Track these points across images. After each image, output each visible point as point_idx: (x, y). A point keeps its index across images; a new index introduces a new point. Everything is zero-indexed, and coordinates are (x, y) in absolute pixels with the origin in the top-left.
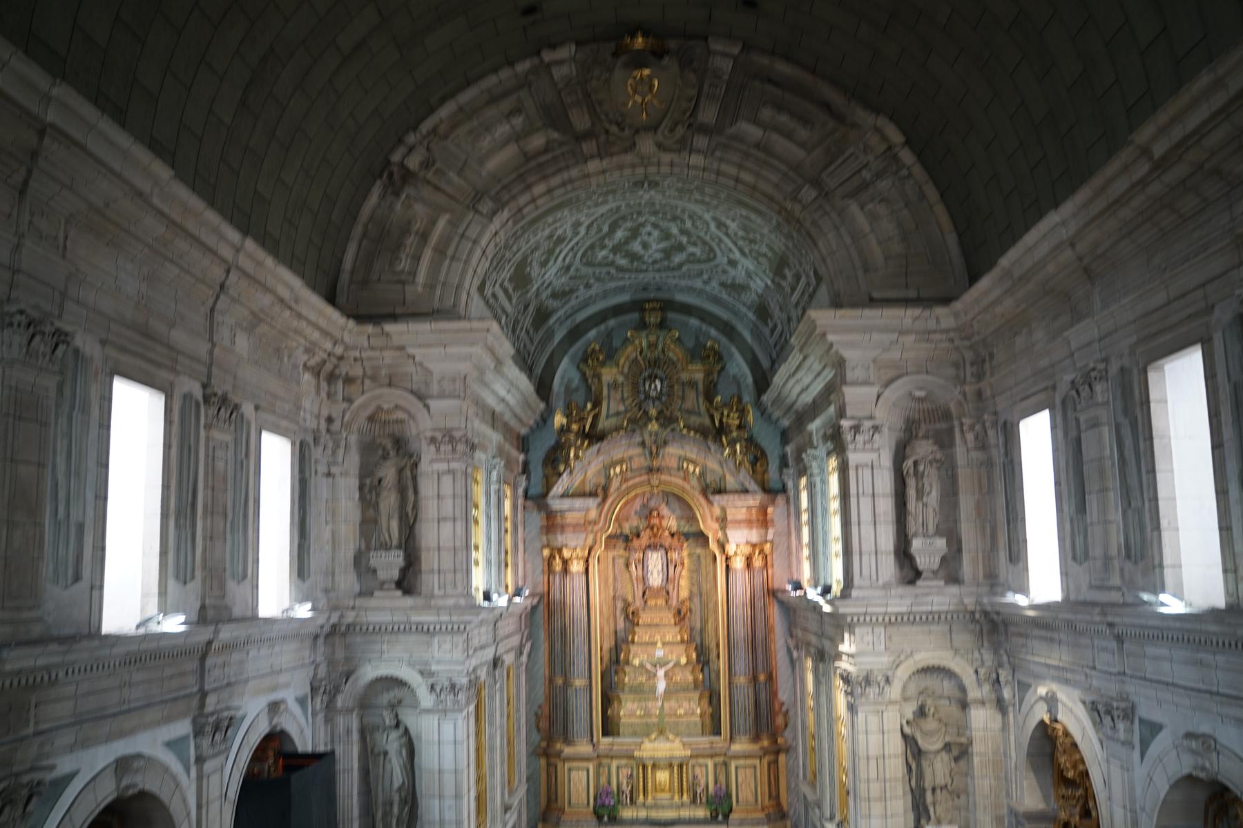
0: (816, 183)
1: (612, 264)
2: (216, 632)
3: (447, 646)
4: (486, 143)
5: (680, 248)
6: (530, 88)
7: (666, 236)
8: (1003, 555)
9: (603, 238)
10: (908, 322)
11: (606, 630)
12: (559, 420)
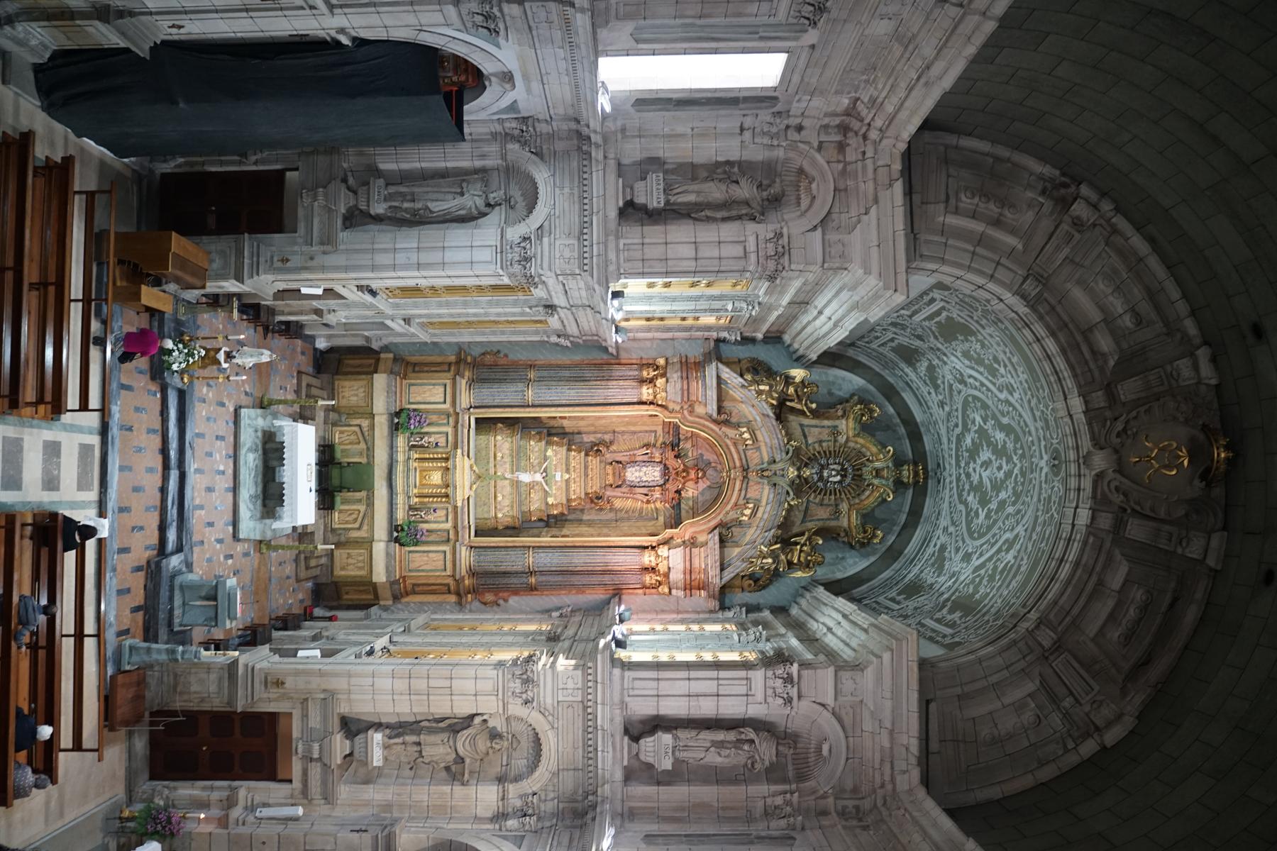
0: (1058, 647)
2: (582, 10)
3: (567, 254)
4: (1102, 286)
5: (984, 502)
6: (1167, 334)
7: (997, 487)
8: (653, 828)
9: (994, 417)
10: (904, 739)
11: (582, 423)
12: (798, 374)
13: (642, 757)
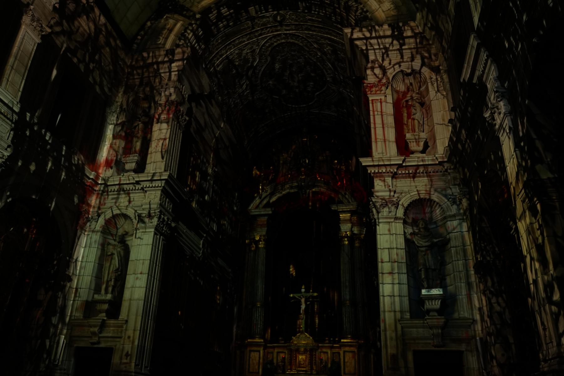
13: (421, 148)
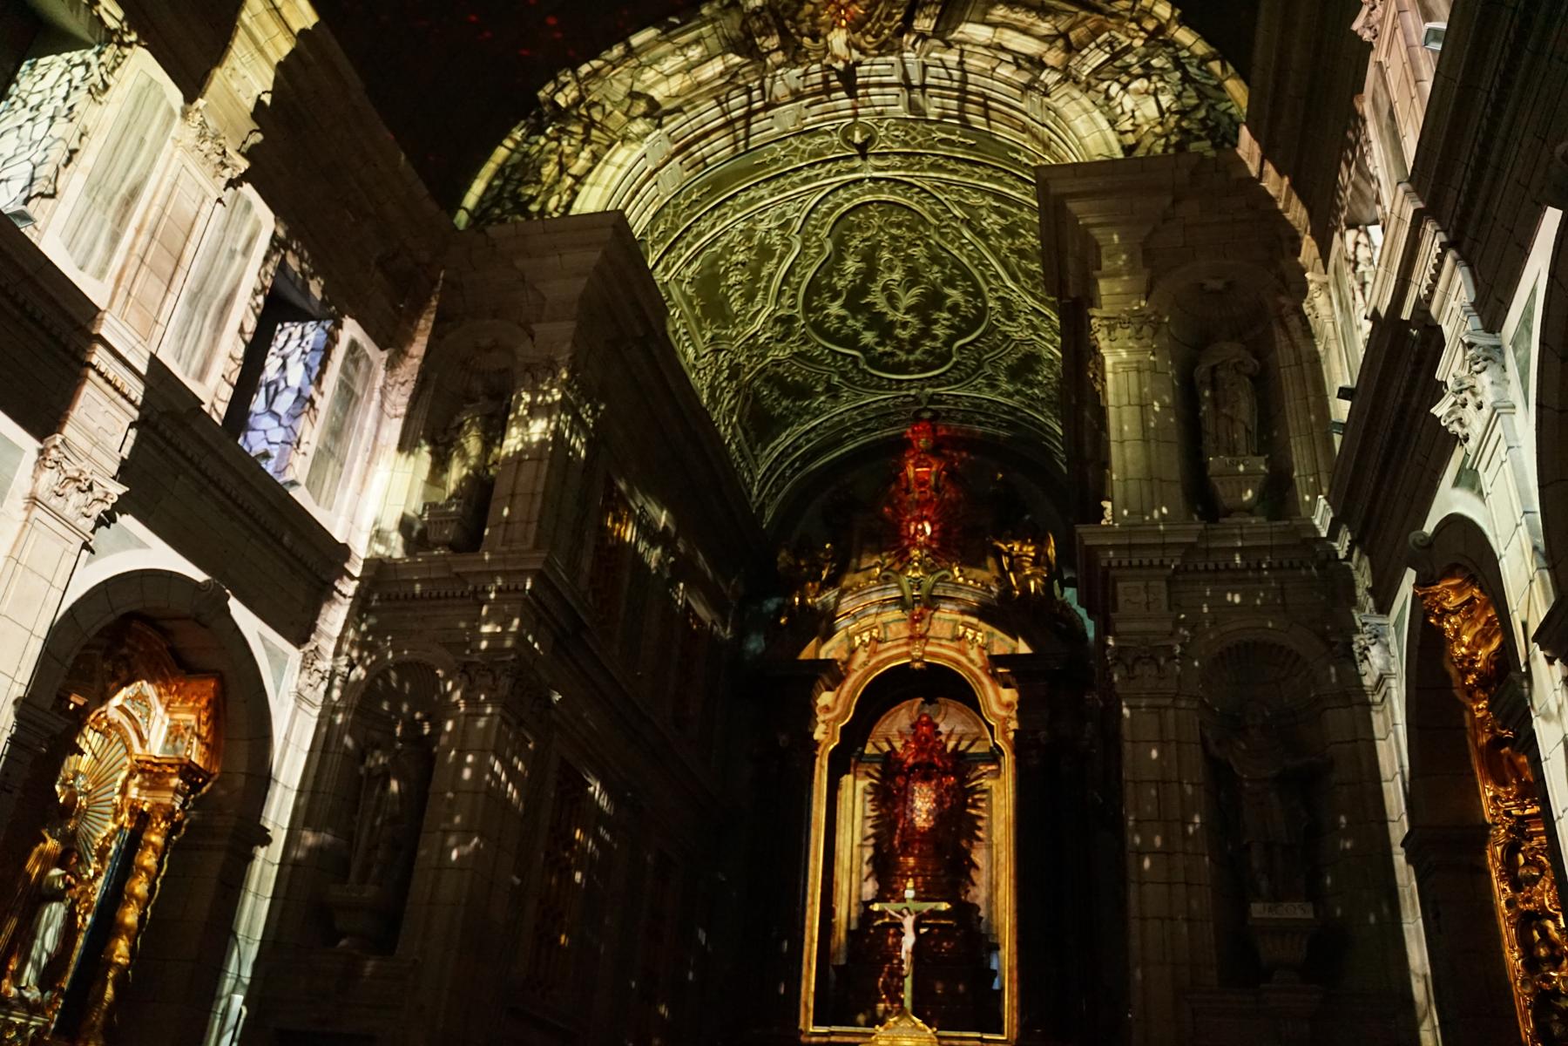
1: (852, 340)
